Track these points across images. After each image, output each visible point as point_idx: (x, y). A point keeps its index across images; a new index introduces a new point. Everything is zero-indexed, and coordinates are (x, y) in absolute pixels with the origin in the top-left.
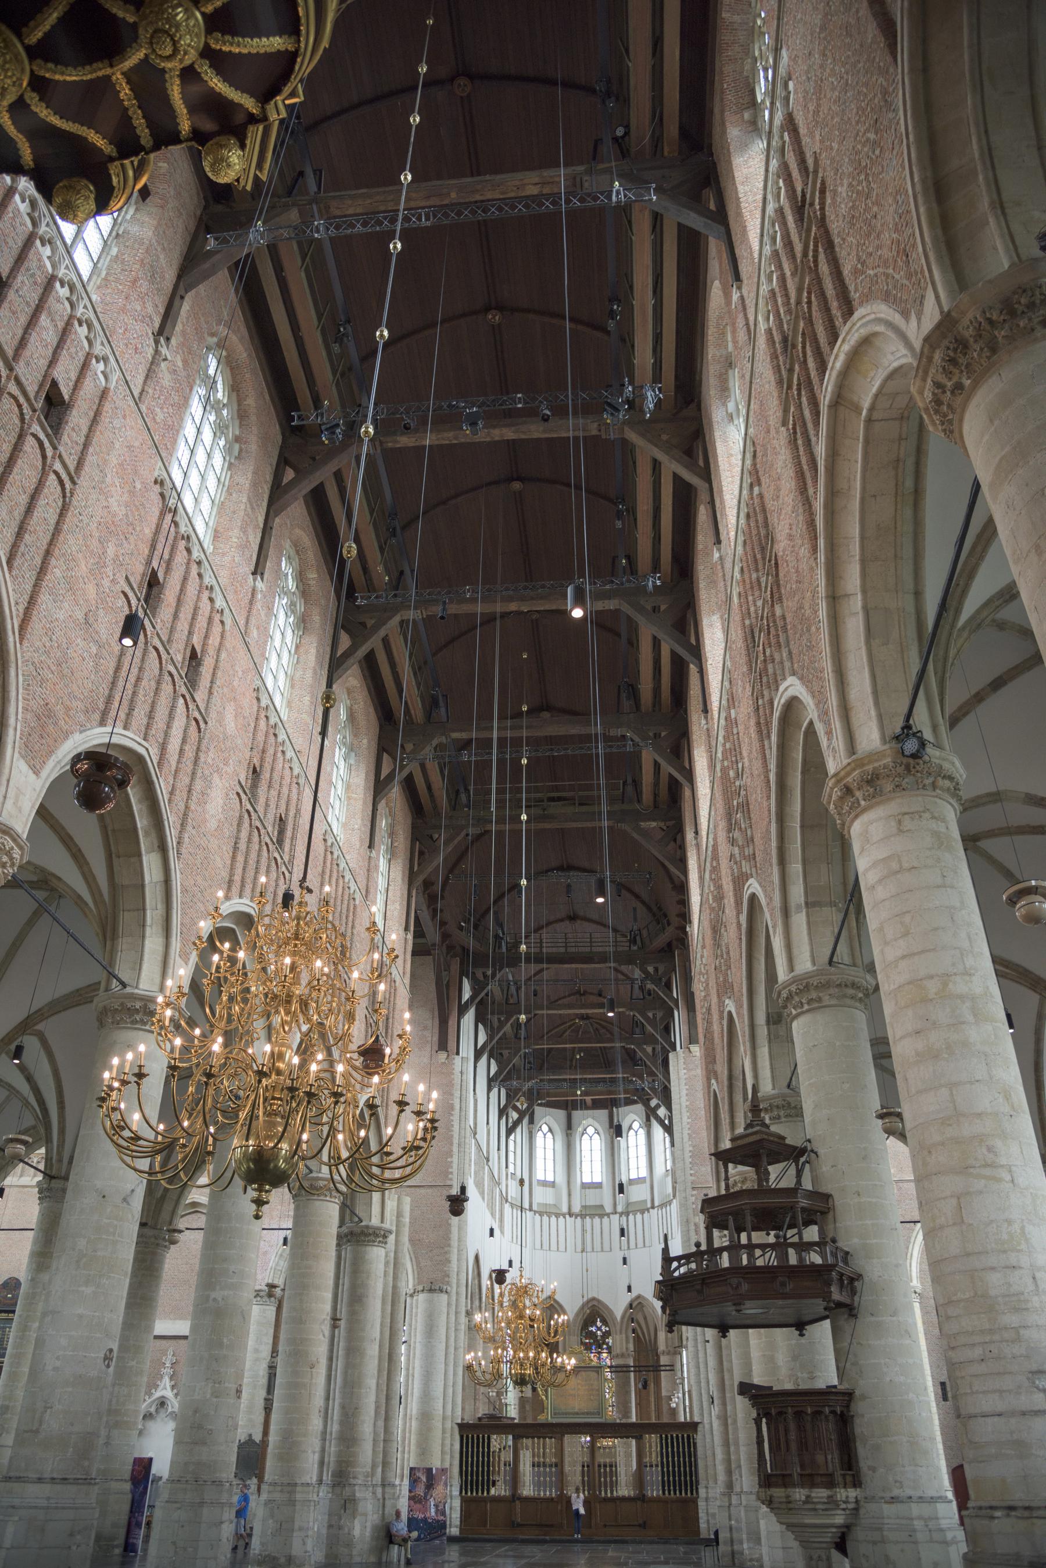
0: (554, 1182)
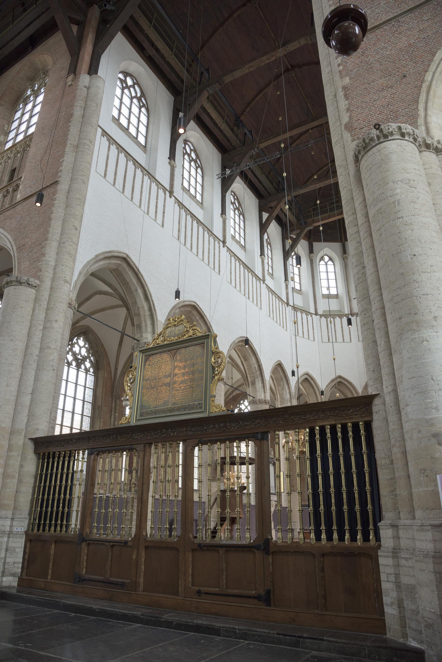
0: (337, 294)
